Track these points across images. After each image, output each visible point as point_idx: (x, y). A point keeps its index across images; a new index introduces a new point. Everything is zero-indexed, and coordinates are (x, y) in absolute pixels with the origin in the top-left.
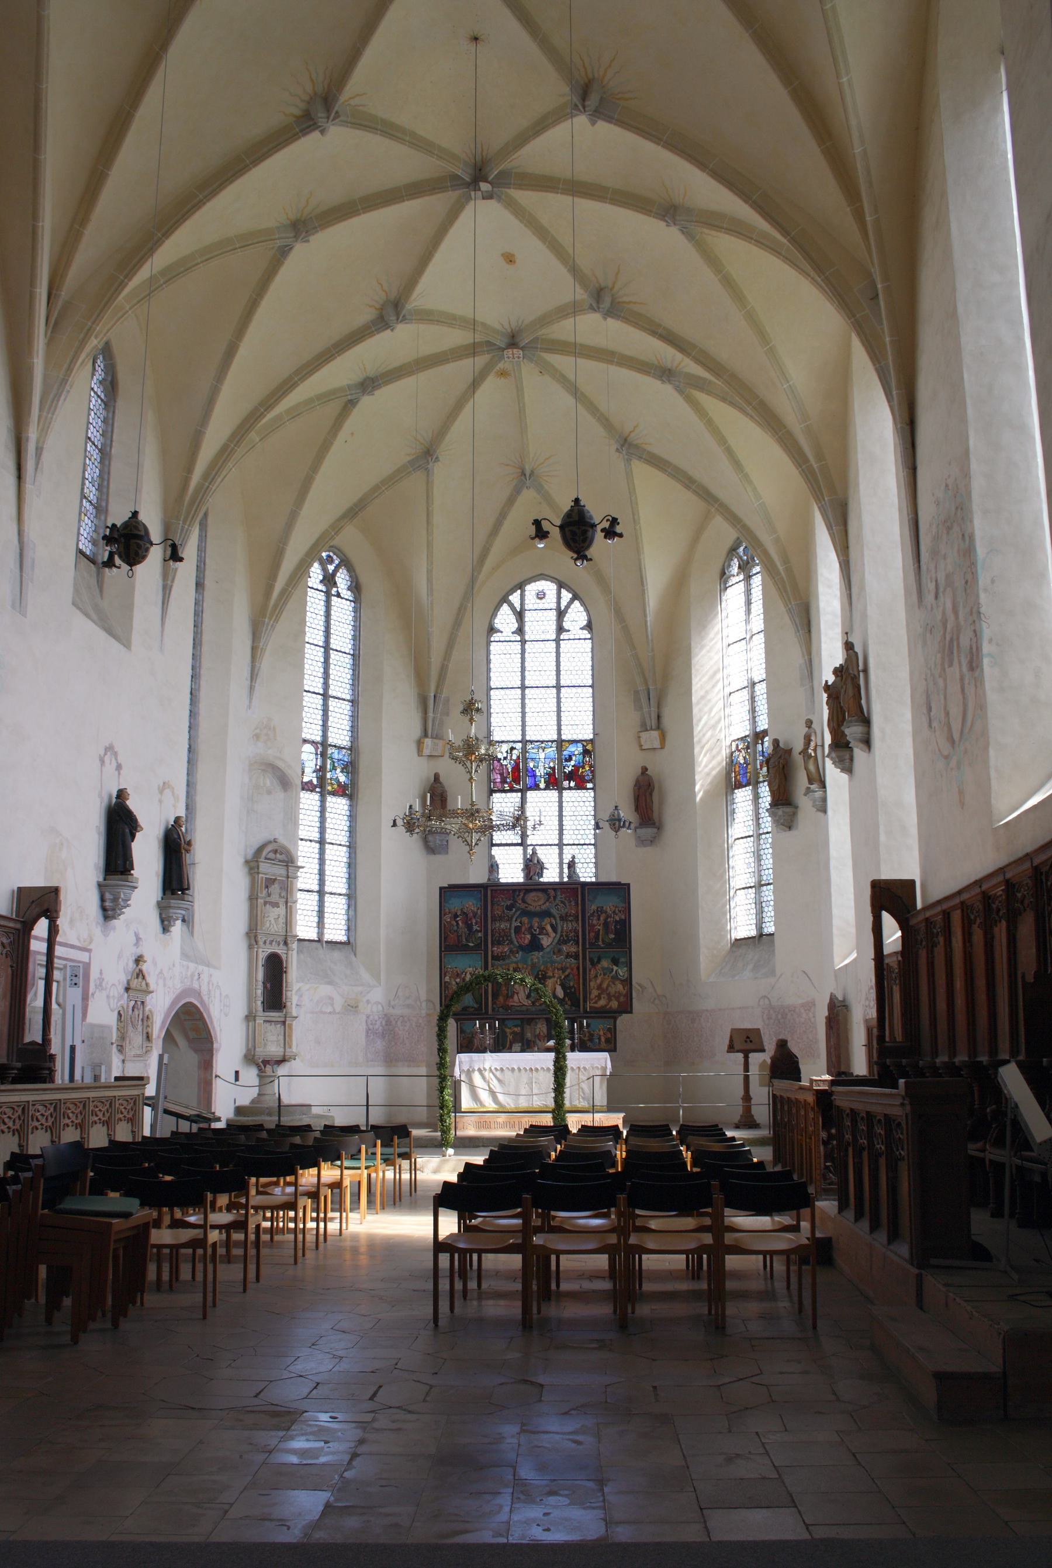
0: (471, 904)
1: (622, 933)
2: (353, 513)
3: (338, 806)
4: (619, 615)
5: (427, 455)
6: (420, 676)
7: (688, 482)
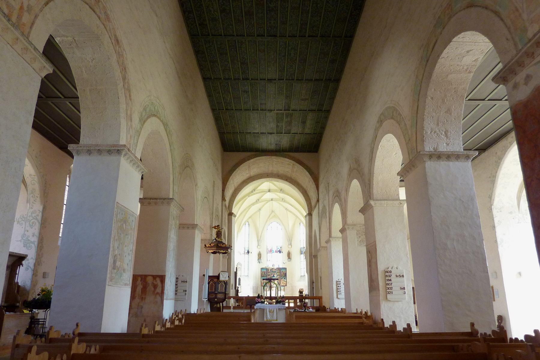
0: (265, 271)
1: (285, 275)
2: (250, 218)
3: (246, 256)
4: (285, 229)
5: (260, 209)
6: (258, 237)
7: (295, 215)
